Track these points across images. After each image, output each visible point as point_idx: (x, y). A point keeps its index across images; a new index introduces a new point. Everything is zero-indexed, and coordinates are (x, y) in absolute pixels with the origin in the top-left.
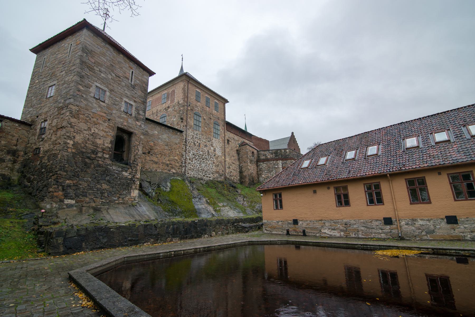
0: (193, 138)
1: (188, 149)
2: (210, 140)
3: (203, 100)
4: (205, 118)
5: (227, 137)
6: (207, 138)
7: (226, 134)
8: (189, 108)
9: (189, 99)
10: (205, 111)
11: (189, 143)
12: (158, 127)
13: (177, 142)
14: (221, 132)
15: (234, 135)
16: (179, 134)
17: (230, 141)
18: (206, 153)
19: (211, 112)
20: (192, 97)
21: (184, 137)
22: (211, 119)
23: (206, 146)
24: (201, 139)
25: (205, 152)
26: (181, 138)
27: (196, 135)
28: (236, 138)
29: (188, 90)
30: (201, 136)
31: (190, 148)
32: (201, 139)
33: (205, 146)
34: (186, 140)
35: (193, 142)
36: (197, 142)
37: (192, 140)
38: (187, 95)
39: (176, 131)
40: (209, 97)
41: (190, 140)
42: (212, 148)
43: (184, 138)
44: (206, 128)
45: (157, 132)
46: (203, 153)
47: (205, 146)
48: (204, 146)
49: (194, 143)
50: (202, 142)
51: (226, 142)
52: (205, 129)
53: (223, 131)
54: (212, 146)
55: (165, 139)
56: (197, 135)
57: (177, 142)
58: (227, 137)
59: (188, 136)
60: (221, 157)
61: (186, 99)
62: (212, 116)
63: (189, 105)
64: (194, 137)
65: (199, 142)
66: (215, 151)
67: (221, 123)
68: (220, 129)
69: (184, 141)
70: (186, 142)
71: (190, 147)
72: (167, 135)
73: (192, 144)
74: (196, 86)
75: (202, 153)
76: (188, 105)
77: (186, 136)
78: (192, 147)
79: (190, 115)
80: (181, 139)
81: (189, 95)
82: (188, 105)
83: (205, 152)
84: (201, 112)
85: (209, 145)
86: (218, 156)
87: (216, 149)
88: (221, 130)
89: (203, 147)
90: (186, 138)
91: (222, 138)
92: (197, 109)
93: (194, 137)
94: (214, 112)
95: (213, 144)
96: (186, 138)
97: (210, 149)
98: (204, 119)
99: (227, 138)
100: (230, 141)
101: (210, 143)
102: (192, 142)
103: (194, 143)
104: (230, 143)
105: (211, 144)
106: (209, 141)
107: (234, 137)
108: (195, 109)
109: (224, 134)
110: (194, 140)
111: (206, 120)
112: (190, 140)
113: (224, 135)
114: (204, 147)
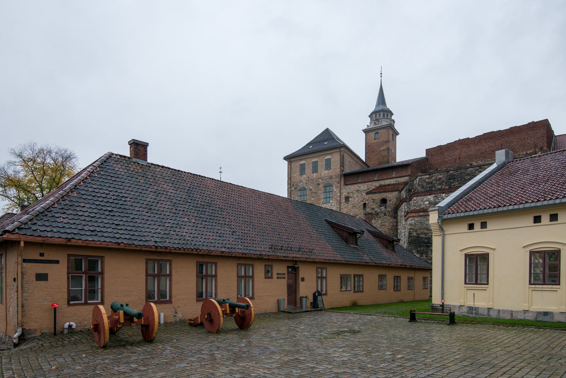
4: (311, 188)
5: (345, 194)
7: (342, 191)
8: (293, 189)
9: (292, 179)
10: (311, 179)
14: (335, 192)
15: (359, 185)
17: (351, 197)
19: (319, 176)
20: (296, 175)
22: (319, 184)
28: (364, 187)
38: (290, 177)
40: (316, 159)
44: (313, 199)
51: (344, 201)
53: (339, 189)
61: (289, 182)
62: (322, 179)
63: (293, 185)
79: (294, 194)
82: (292, 186)
88: (335, 190)
91: (336, 200)
98: (311, 190)
99: (346, 195)
104: (350, 199)
107: (360, 186)
108: (299, 185)
109: (340, 193)
113: (339, 194)
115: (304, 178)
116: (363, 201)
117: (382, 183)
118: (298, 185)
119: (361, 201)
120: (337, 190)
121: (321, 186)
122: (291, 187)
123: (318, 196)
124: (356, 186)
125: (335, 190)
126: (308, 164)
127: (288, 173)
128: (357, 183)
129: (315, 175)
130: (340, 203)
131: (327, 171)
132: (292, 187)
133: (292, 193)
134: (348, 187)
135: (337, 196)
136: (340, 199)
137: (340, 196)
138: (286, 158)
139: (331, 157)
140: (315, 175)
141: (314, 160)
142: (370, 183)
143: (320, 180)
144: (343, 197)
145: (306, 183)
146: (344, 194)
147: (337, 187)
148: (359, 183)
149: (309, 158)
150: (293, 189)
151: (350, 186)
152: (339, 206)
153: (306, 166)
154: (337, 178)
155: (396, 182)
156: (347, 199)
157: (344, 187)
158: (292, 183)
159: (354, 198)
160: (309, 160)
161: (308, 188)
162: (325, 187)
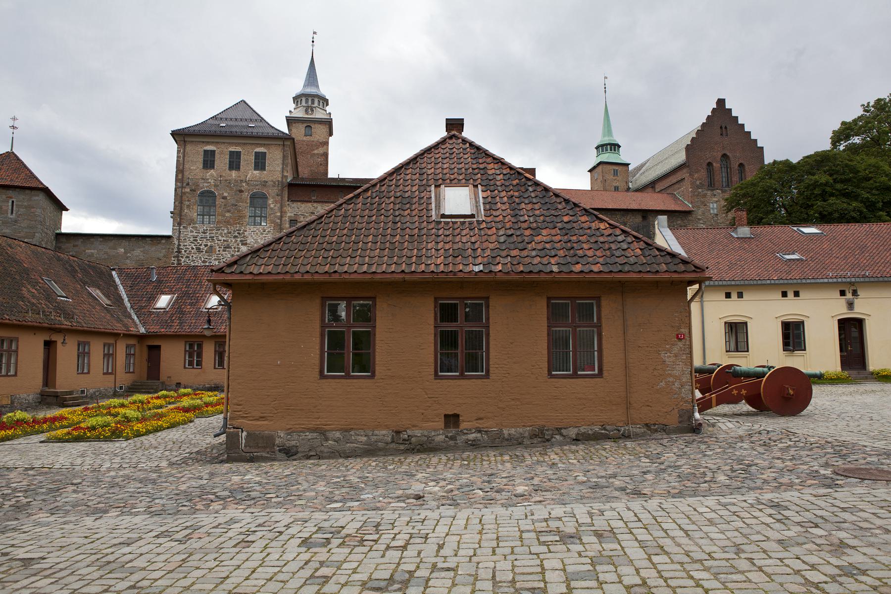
1: (184, 261)
2: (238, 233)
3: (222, 162)
4: (225, 194)
5: (290, 214)
6: (230, 233)
7: (285, 209)
8: (188, 190)
9: (186, 174)
10: (226, 180)
11: (185, 251)
12: (124, 241)
13: (161, 255)
14: (271, 209)
15: (315, 205)
16: (163, 241)
19: (243, 178)
21: (175, 244)
22: (241, 191)
24: (215, 238)
26: (168, 247)
27: (202, 233)
29: (184, 159)
31: (189, 260)
32: (215, 238)
33: (224, 248)
34: (178, 248)
35: (194, 247)
36: (206, 246)
37: (193, 245)
41: (189, 245)
43: (176, 246)
44: (228, 215)
45: (122, 250)
46: (219, 262)
47: (224, 248)
48: (221, 249)
49: (198, 249)
50: (217, 242)
52: (224, 216)
53: (278, 205)
54: (245, 244)
55: (137, 256)
56: (204, 233)
57: (161, 255)
59: (185, 239)
61: (180, 177)
63: (188, 184)
64: (198, 239)
65: (209, 244)
67: (272, 193)
69: (176, 250)
70: (179, 252)
71: (187, 257)
72: (142, 249)
74: (203, 142)
76: (185, 185)
77: (179, 242)
78: (192, 256)
80: (169, 249)
81: (187, 166)
82: (185, 185)
84: (216, 186)
85: (235, 245)
89: (219, 251)
90: (179, 245)
91: (273, 222)
92: (206, 184)
93: (198, 239)
94: (253, 174)
95: (246, 240)
96: (179, 245)
98: (224, 198)
101: (239, 239)
102: (193, 249)
103: (198, 249)
105: (241, 241)
106: (235, 237)
107: (317, 207)
108: (201, 185)
109: (281, 212)
110: (199, 243)
111: (228, 198)
112: (189, 245)
114: (223, 251)
115: (212, 175)
118: (199, 186)
120: (275, 206)
121: (246, 195)
122: (182, 187)
124: (309, 205)
125: (272, 206)
126: (221, 153)
127: (178, 161)
128: (311, 202)
129: (234, 174)
131: (258, 172)
132: (185, 188)
133: (185, 197)
134: (295, 205)
135: (276, 217)
136: (281, 222)
137: (281, 217)
138: (175, 134)
139: (265, 151)
140: (234, 175)
141: (232, 149)
143: (244, 184)
145: (216, 186)
146: (289, 214)
147: (276, 202)
148: (315, 202)
150: (188, 190)
151: (299, 203)
153: (217, 156)
154: (274, 186)
157: (288, 203)
158: (184, 179)
160: (223, 146)
161: (219, 194)
162: (253, 197)
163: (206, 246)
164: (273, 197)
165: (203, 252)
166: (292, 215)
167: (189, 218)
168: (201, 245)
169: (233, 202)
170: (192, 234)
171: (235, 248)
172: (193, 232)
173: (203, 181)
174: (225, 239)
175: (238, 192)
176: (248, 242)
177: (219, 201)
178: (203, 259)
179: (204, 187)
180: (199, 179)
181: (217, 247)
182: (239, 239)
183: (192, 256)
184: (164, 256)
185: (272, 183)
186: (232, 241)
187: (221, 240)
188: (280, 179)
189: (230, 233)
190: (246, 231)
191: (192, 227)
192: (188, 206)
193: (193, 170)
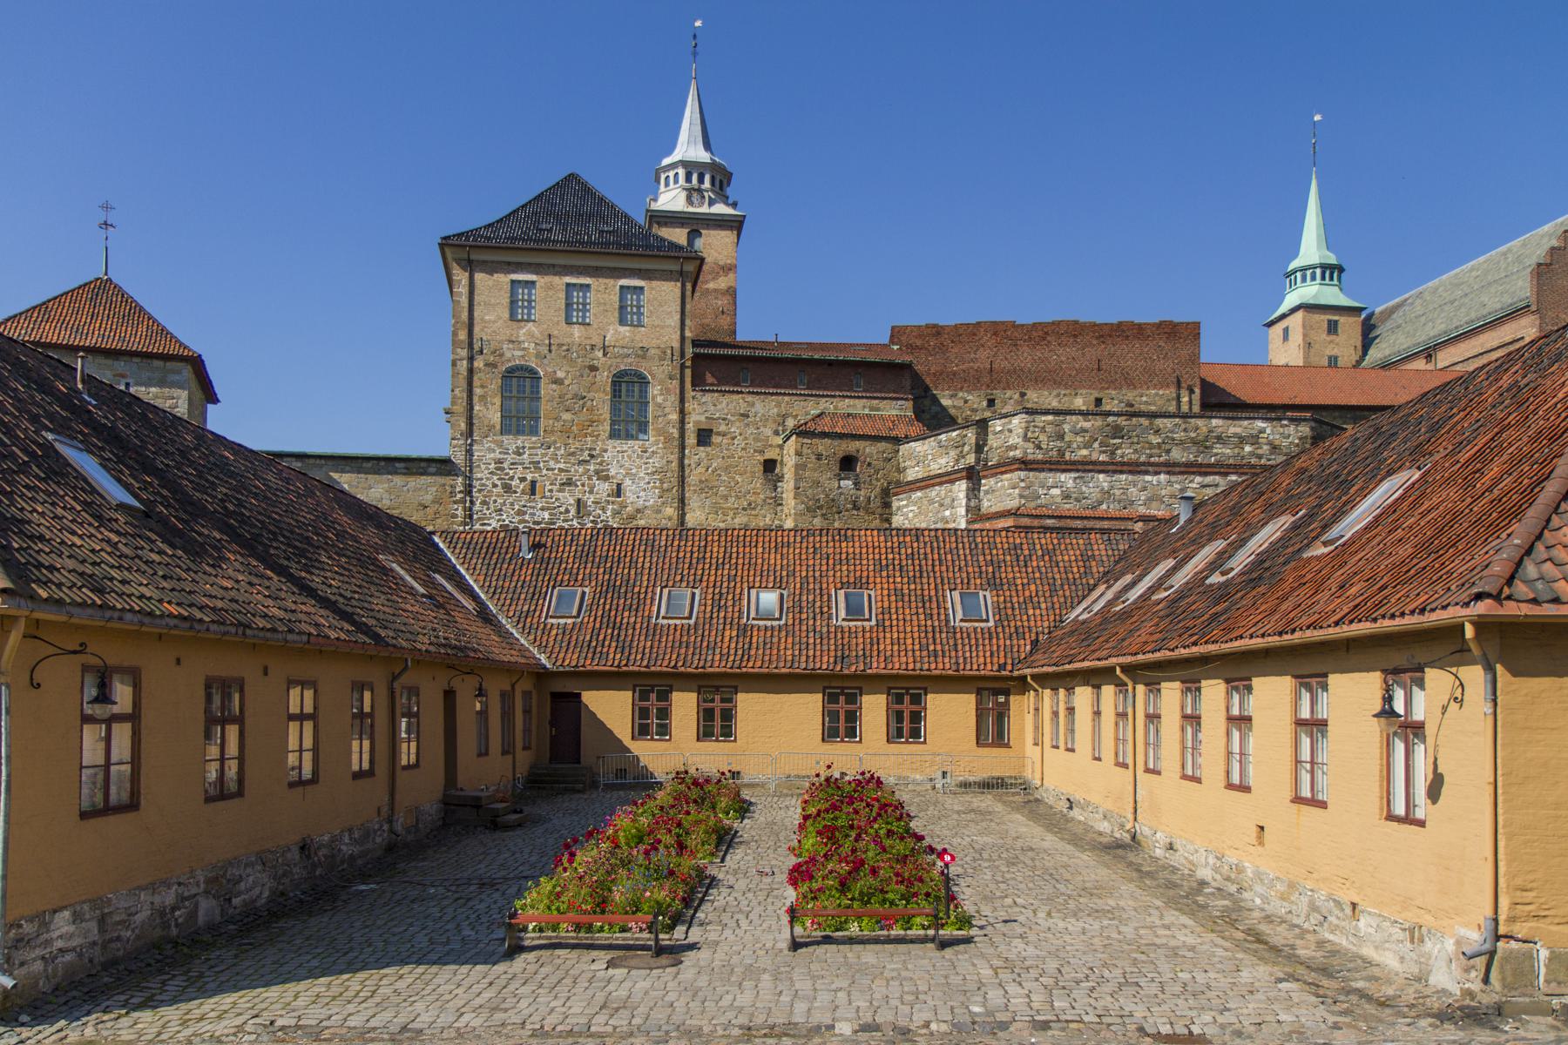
0: (502, 469)
4: (560, 374)
5: (696, 418)
6: (573, 454)
9: (477, 329)
10: (560, 345)
14: (659, 406)
15: (750, 398)
17: (718, 434)
18: (567, 511)
19: (596, 340)
22: (593, 369)
23: (569, 483)
25: (562, 509)
27: (514, 453)
30: (539, 452)
32: (542, 465)
33: (563, 484)
35: (499, 483)
39: (423, 464)
41: (488, 479)
42: (603, 488)
44: (567, 416)
46: (550, 514)
49: (508, 489)
50: (544, 472)
51: (691, 439)
52: (557, 419)
54: (607, 478)
56: (520, 454)
58: (696, 418)
60: (658, 512)
64: (505, 465)
66: (618, 491)
68: (654, 398)
73: (499, 489)
74: (509, 263)
75: (546, 515)
83: (562, 509)
85: (585, 478)
86: (638, 511)
87: (628, 482)
89: (551, 491)
91: (660, 432)
92: (519, 353)
93: (505, 465)
94: (618, 333)
97: (591, 492)
98: (558, 382)
100: (718, 434)
102: (495, 486)
103: (508, 489)
104: (716, 439)
107: (753, 405)
108: (508, 355)
110: (507, 474)
111: (567, 382)
112: (488, 479)
113: (674, 417)
116: (762, 452)
117: (826, 405)
118: (502, 355)
119: (755, 451)
121: (604, 378)
123: (591, 410)
125: (659, 399)
129: (577, 331)
130: (682, 447)
134: (708, 398)
140: (577, 335)
142: (786, 398)
144: (690, 427)
149: (554, 266)
152: (674, 457)
155: (872, 409)
156: (704, 437)
157: (693, 394)
159: (733, 438)
163: (523, 479)
164: (661, 383)
165: (515, 492)
166: (703, 418)
167: (486, 423)
168: (512, 478)
169: (574, 388)
170: (492, 455)
171: (583, 485)
172: (494, 451)
173: (511, 346)
174: (562, 466)
175: (587, 371)
176: (612, 472)
177: (546, 389)
178: (517, 507)
179: (514, 357)
180: (501, 342)
181: (548, 483)
182: (592, 468)
183: (495, 501)
184: (433, 502)
185: (657, 352)
186: (576, 471)
187: (553, 469)
188: (676, 345)
189: (573, 454)
190: (606, 451)
191: (494, 442)
192: (483, 398)
193: (490, 321)
